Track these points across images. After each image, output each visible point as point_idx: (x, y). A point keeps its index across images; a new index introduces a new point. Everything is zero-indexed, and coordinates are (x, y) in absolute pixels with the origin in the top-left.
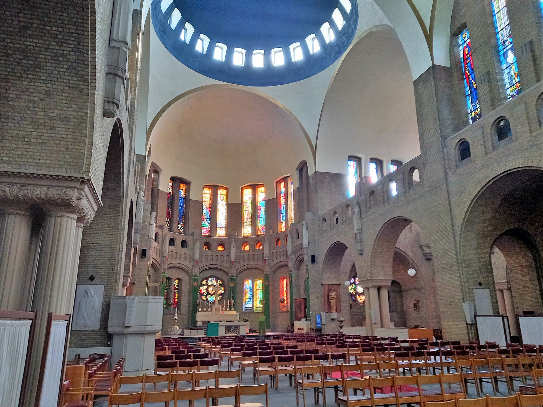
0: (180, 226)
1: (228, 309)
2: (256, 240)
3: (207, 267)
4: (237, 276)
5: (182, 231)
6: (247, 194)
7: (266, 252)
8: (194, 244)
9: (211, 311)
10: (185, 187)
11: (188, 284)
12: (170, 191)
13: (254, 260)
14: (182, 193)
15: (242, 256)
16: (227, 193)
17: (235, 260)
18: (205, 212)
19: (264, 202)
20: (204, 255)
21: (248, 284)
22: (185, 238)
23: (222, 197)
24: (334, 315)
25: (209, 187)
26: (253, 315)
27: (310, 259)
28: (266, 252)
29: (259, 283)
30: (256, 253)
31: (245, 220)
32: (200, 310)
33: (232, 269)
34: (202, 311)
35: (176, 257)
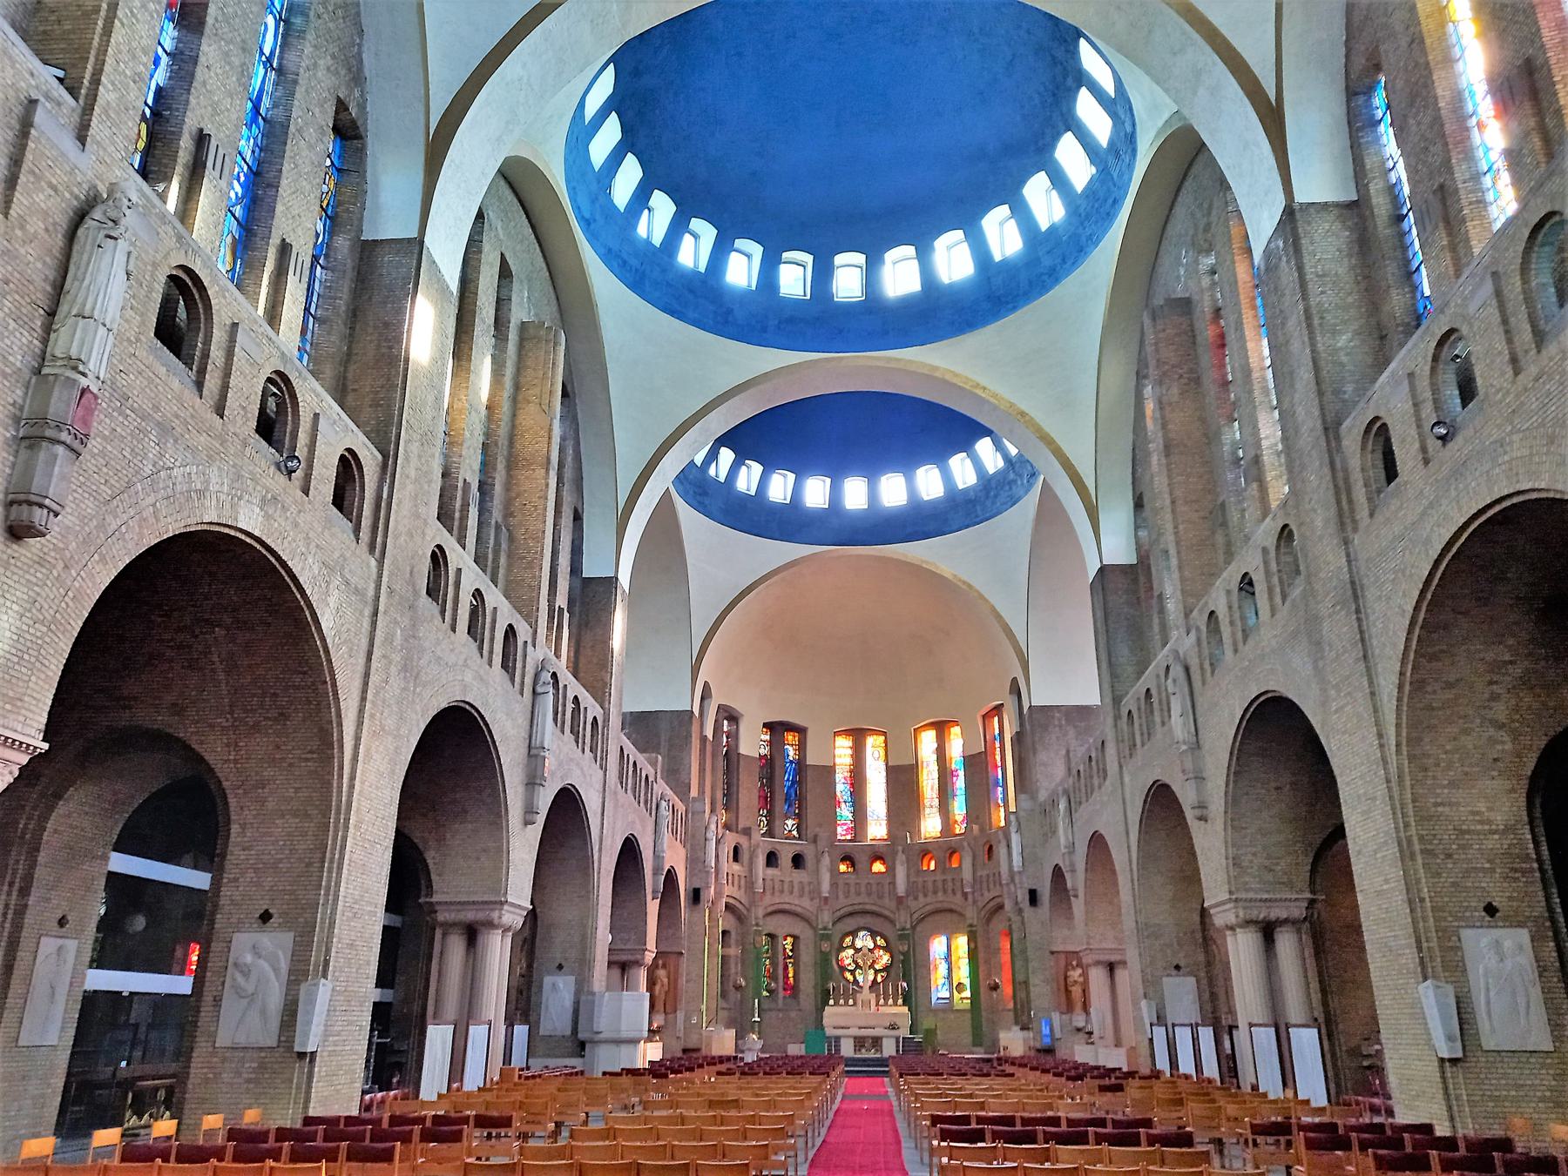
0: (790, 822)
1: (891, 1001)
2: (947, 848)
3: (850, 909)
4: (914, 928)
5: (795, 833)
6: (928, 740)
7: (967, 874)
8: (818, 861)
11: (811, 947)
12: (764, 751)
13: (945, 891)
14: (791, 752)
15: (920, 886)
16: (886, 742)
17: (907, 891)
18: (842, 788)
20: (841, 882)
21: (938, 946)
22: (798, 848)
24: (1079, 1020)
25: (847, 733)
27: (1027, 897)
28: (967, 874)
29: (961, 943)
30: (949, 878)
31: (927, 804)
32: (831, 1002)
33: (902, 912)
34: (836, 1004)
35: (782, 891)
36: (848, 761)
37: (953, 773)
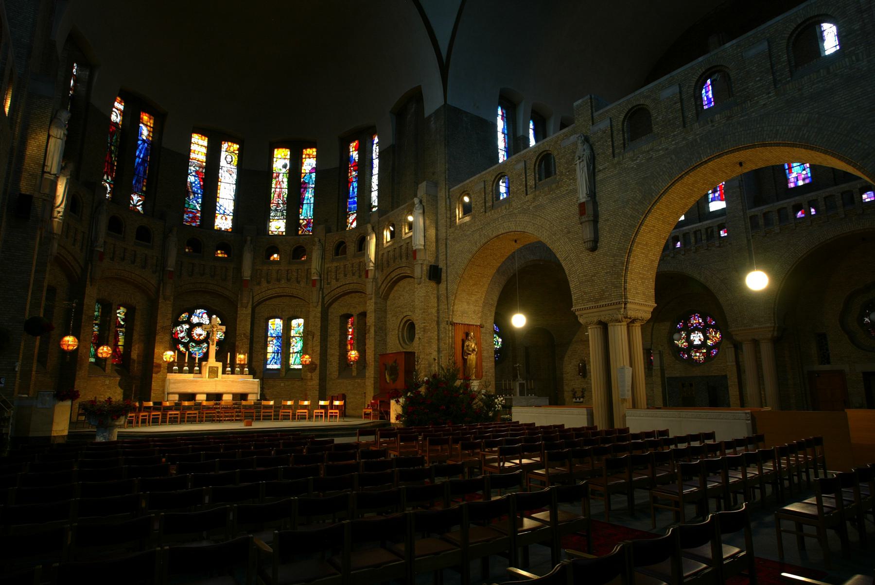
9: (200, 372)
10: (152, 121)
13: (288, 280)
17: (251, 277)
19: (313, 175)
21: (275, 325)
23: (229, 157)
26: (282, 384)
36: (202, 158)
37: (304, 186)
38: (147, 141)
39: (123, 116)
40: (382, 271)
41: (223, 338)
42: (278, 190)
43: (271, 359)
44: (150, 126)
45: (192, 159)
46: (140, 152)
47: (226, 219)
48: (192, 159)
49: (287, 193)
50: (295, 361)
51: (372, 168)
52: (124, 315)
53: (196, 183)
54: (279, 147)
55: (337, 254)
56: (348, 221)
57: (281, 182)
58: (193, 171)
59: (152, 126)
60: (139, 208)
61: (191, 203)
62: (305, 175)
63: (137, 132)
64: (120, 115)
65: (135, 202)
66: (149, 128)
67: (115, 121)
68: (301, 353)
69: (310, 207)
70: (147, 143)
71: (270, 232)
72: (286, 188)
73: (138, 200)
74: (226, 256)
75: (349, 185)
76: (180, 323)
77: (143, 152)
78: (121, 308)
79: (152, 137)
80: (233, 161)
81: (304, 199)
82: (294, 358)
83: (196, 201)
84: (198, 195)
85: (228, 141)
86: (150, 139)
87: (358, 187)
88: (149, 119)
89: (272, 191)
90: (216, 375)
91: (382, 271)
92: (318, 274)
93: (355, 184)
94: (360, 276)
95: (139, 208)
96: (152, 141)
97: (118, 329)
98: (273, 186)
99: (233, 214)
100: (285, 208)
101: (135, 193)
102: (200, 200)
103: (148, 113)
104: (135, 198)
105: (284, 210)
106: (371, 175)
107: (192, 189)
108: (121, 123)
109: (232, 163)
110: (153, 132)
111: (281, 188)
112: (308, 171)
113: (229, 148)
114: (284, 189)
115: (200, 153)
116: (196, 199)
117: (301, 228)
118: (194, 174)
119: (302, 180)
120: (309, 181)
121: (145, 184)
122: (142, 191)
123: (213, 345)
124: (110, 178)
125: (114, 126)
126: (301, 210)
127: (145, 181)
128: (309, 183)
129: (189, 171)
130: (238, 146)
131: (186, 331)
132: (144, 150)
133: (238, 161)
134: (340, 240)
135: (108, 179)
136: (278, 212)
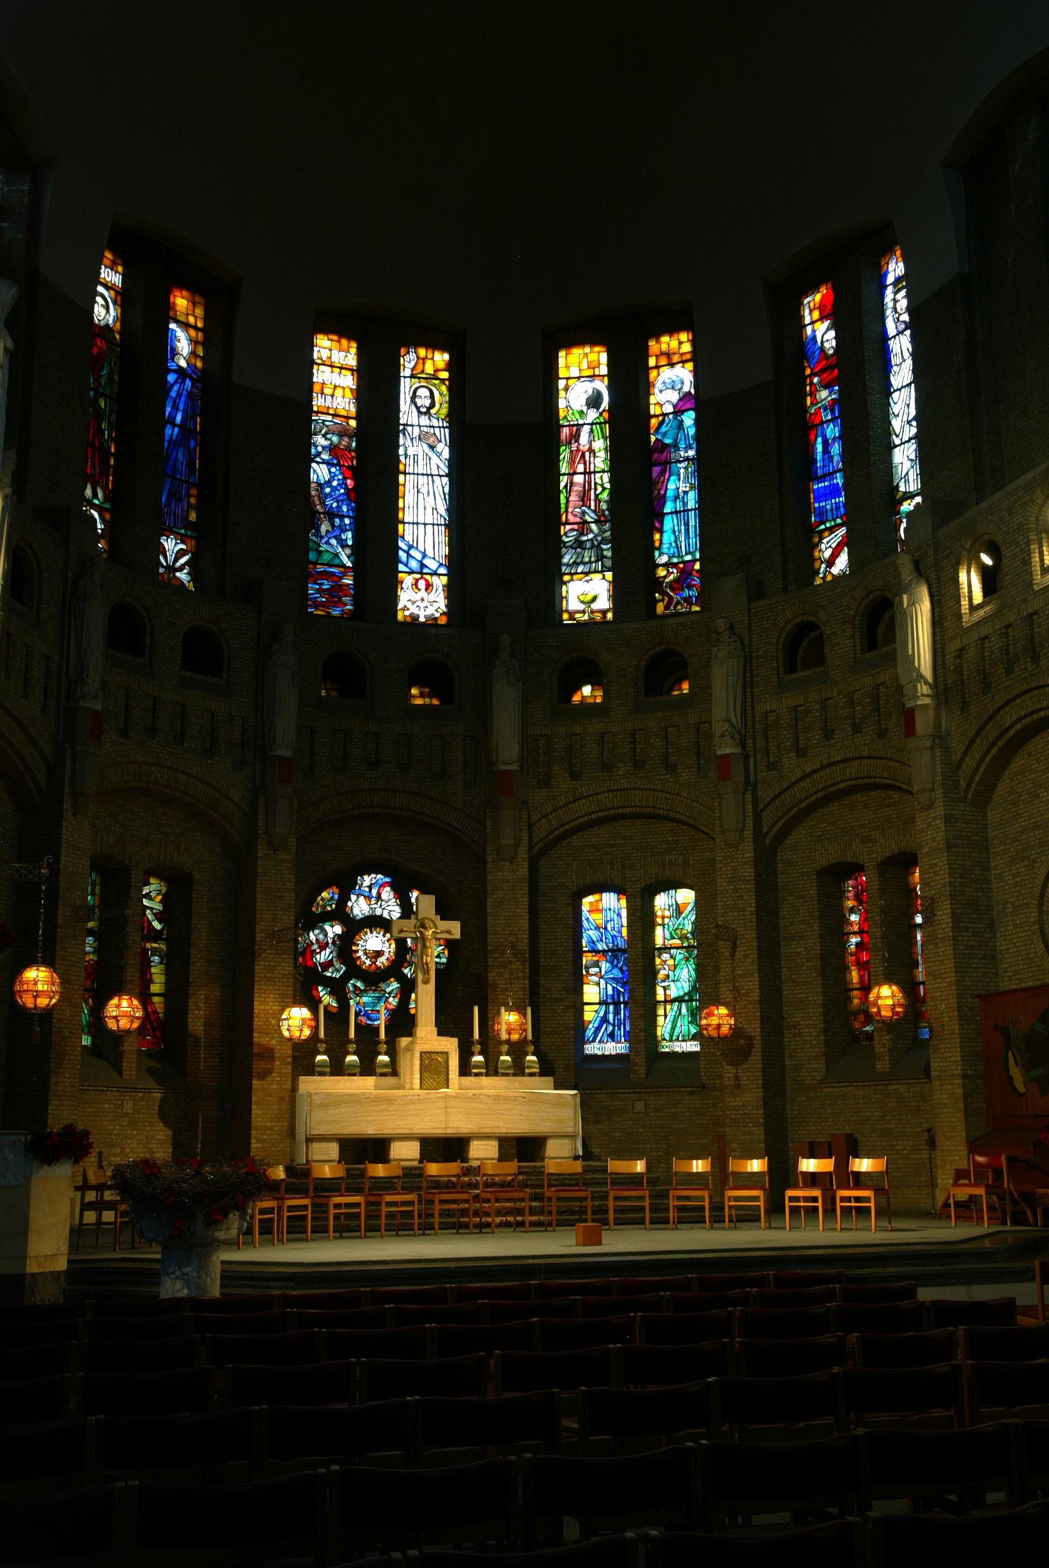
9: (393, 1070)
10: (199, 312)
13: (638, 764)
19: (689, 419)
26: (640, 1106)
38: (190, 371)
39: (122, 307)
40: (964, 707)
41: (444, 960)
42: (579, 479)
43: (596, 1025)
44: (195, 328)
45: (318, 413)
46: (175, 408)
47: (428, 586)
48: (318, 413)
49: (608, 486)
50: (673, 1029)
51: (886, 367)
52: (161, 902)
53: (335, 483)
54: (569, 345)
55: (792, 668)
56: (816, 554)
57: (587, 454)
58: (324, 448)
59: (200, 325)
60: (183, 576)
61: (324, 547)
62: (661, 424)
63: (164, 347)
64: (115, 303)
65: (171, 557)
66: (192, 333)
67: (102, 323)
68: (691, 1000)
69: (687, 525)
70: (192, 379)
71: (565, 616)
72: (603, 471)
73: (178, 552)
74: (436, 702)
75: (812, 437)
76: (315, 921)
77: (181, 406)
78: (152, 880)
79: (202, 359)
80: (437, 405)
81: (663, 500)
82: (670, 1018)
83: (338, 538)
84: (342, 520)
85: (416, 345)
86: (199, 364)
87: (842, 437)
88: (191, 307)
89: (562, 485)
90: (443, 1077)
91: (964, 707)
92: (736, 736)
93: (832, 431)
94: (882, 734)
95: (183, 576)
96: (203, 370)
97: (148, 945)
98: (564, 468)
99: (449, 568)
100: (608, 534)
101: (168, 532)
102: (349, 535)
103: (188, 289)
104: (171, 545)
105: (604, 541)
106: (887, 390)
107: (323, 503)
108: (118, 325)
109: (433, 411)
110: (204, 344)
111: (590, 473)
112: (668, 409)
113: (420, 367)
114: (598, 475)
115: (339, 392)
116: (337, 533)
117: (664, 593)
118: (325, 456)
119: (653, 439)
120: (675, 440)
121: (193, 501)
122: (188, 525)
123: (426, 982)
124: (100, 494)
125: (102, 339)
126: (657, 536)
127: (194, 492)
128: (675, 446)
129: (313, 451)
130: (446, 357)
131: (334, 943)
132: (183, 399)
133: (450, 403)
134: (800, 619)
135: (95, 495)
136: (585, 549)
